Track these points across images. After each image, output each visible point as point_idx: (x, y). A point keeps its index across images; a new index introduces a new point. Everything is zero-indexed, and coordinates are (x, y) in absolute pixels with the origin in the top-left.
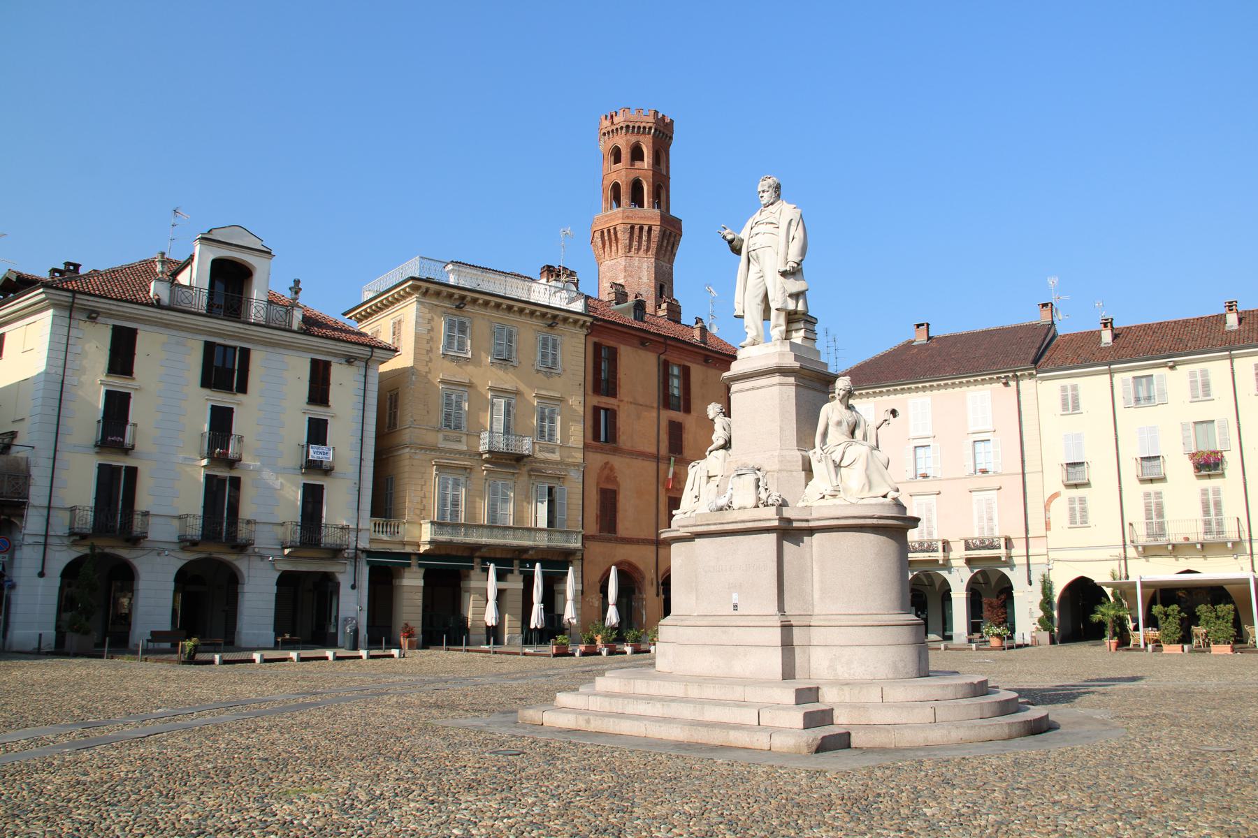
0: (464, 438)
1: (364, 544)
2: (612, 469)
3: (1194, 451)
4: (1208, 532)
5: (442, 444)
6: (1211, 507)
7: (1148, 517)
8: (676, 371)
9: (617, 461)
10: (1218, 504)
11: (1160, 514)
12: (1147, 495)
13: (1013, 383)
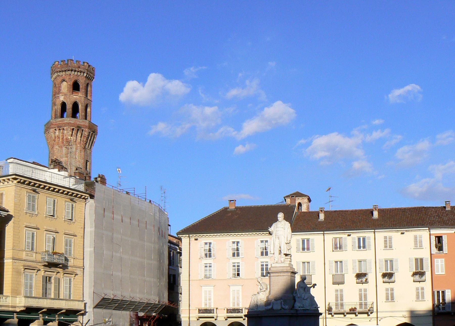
0: (34, 255)
3: (358, 272)
6: (363, 296)
7: (337, 300)
10: (365, 296)
11: (342, 300)
12: (337, 291)
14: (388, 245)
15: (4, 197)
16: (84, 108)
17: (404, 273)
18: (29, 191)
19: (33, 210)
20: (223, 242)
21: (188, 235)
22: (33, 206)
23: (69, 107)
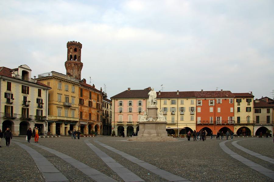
1: (47, 119)
4: (172, 122)
5: (58, 104)
6: (173, 119)
13: (145, 100)
14: (182, 103)
15: (50, 84)
16: (78, 57)
17: (187, 112)
20: (126, 102)
22: (61, 87)
23: (73, 57)
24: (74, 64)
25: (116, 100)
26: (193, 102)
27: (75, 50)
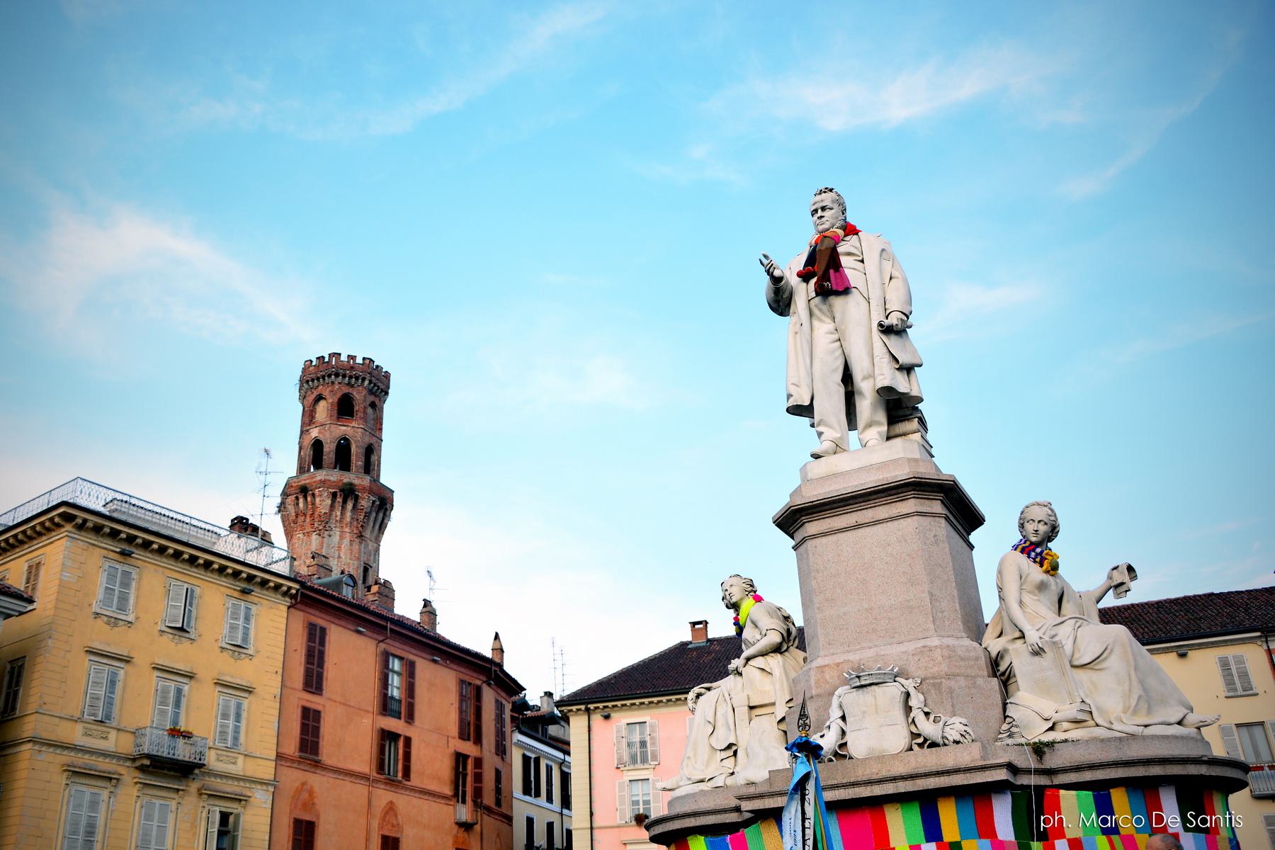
2: (311, 793)
8: (396, 665)
9: (318, 781)
18: (112, 555)
19: (122, 607)
21: (583, 707)
22: (123, 599)
23: (329, 449)
24: (334, 495)
25: (597, 718)
26: (1244, 675)
27: (345, 408)
